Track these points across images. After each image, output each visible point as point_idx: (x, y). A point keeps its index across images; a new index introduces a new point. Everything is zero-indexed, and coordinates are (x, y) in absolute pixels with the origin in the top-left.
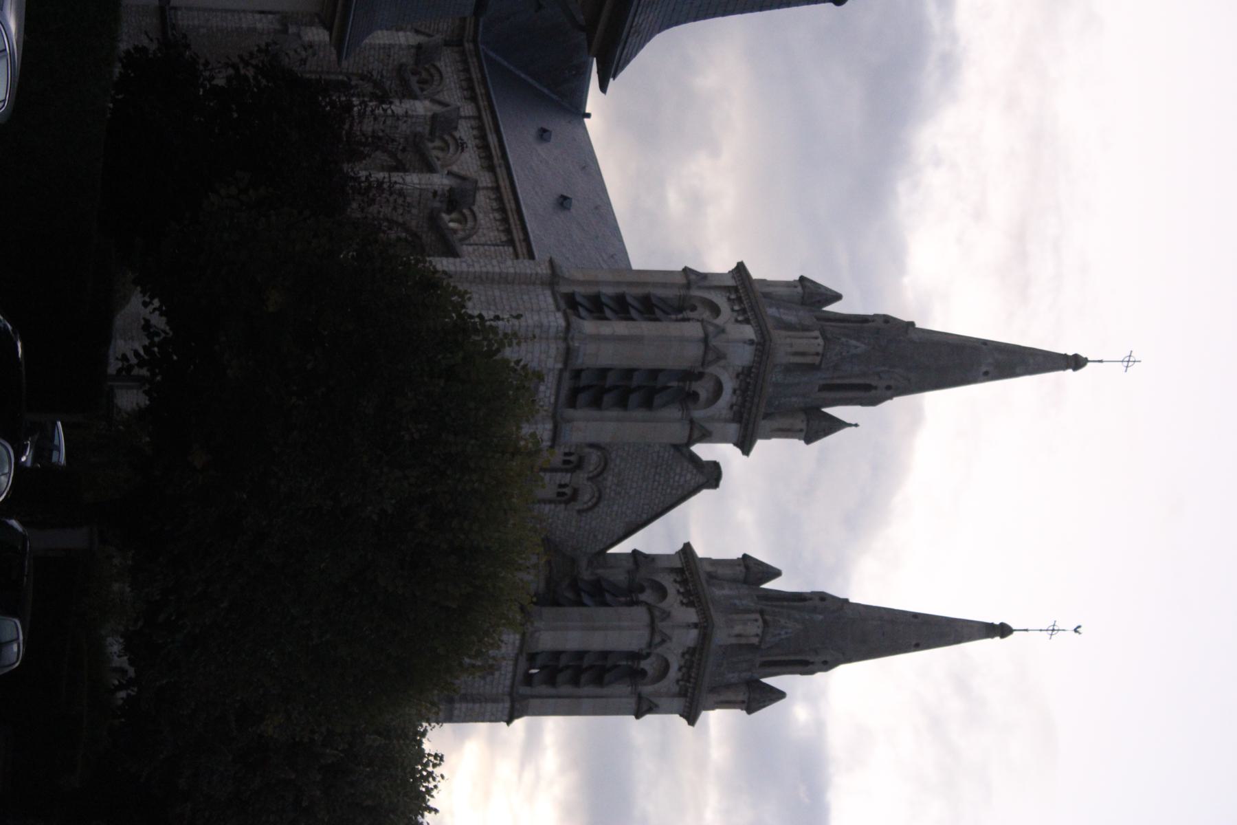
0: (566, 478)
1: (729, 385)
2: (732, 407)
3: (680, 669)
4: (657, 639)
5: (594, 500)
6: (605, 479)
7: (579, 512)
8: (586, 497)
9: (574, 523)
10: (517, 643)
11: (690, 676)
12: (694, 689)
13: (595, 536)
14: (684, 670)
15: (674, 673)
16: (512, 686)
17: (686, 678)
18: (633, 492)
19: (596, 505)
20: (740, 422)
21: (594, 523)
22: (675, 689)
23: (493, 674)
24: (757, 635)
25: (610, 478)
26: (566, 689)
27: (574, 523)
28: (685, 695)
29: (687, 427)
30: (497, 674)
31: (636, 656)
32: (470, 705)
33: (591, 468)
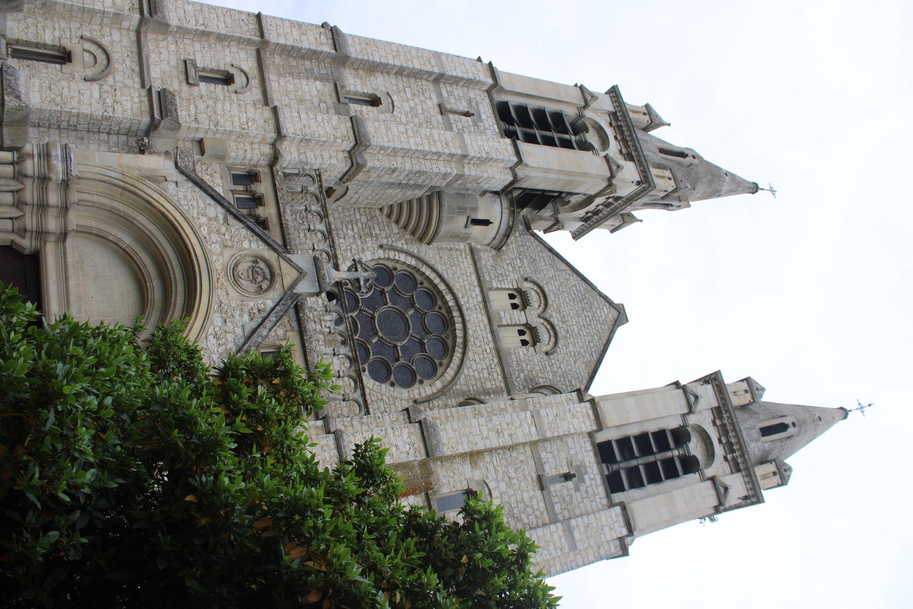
0: (519, 317)
1: (610, 132)
2: (621, 152)
3: (720, 441)
4: (692, 399)
5: (553, 339)
6: (551, 316)
7: (547, 353)
8: (544, 335)
9: (548, 369)
10: (590, 412)
11: (730, 444)
12: (743, 455)
13: (570, 381)
14: (724, 440)
15: (719, 450)
16: (608, 497)
17: (729, 447)
18: (576, 328)
19: (556, 343)
20: (634, 161)
21: (563, 367)
22: (728, 470)
23: (582, 480)
24: (746, 391)
25: (554, 314)
26: (651, 488)
27: (548, 369)
28: (739, 470)
29: (604, 160)
30: (586, 477)
31: (681, 436)
32: (585, 518)
33: (536, 305)
